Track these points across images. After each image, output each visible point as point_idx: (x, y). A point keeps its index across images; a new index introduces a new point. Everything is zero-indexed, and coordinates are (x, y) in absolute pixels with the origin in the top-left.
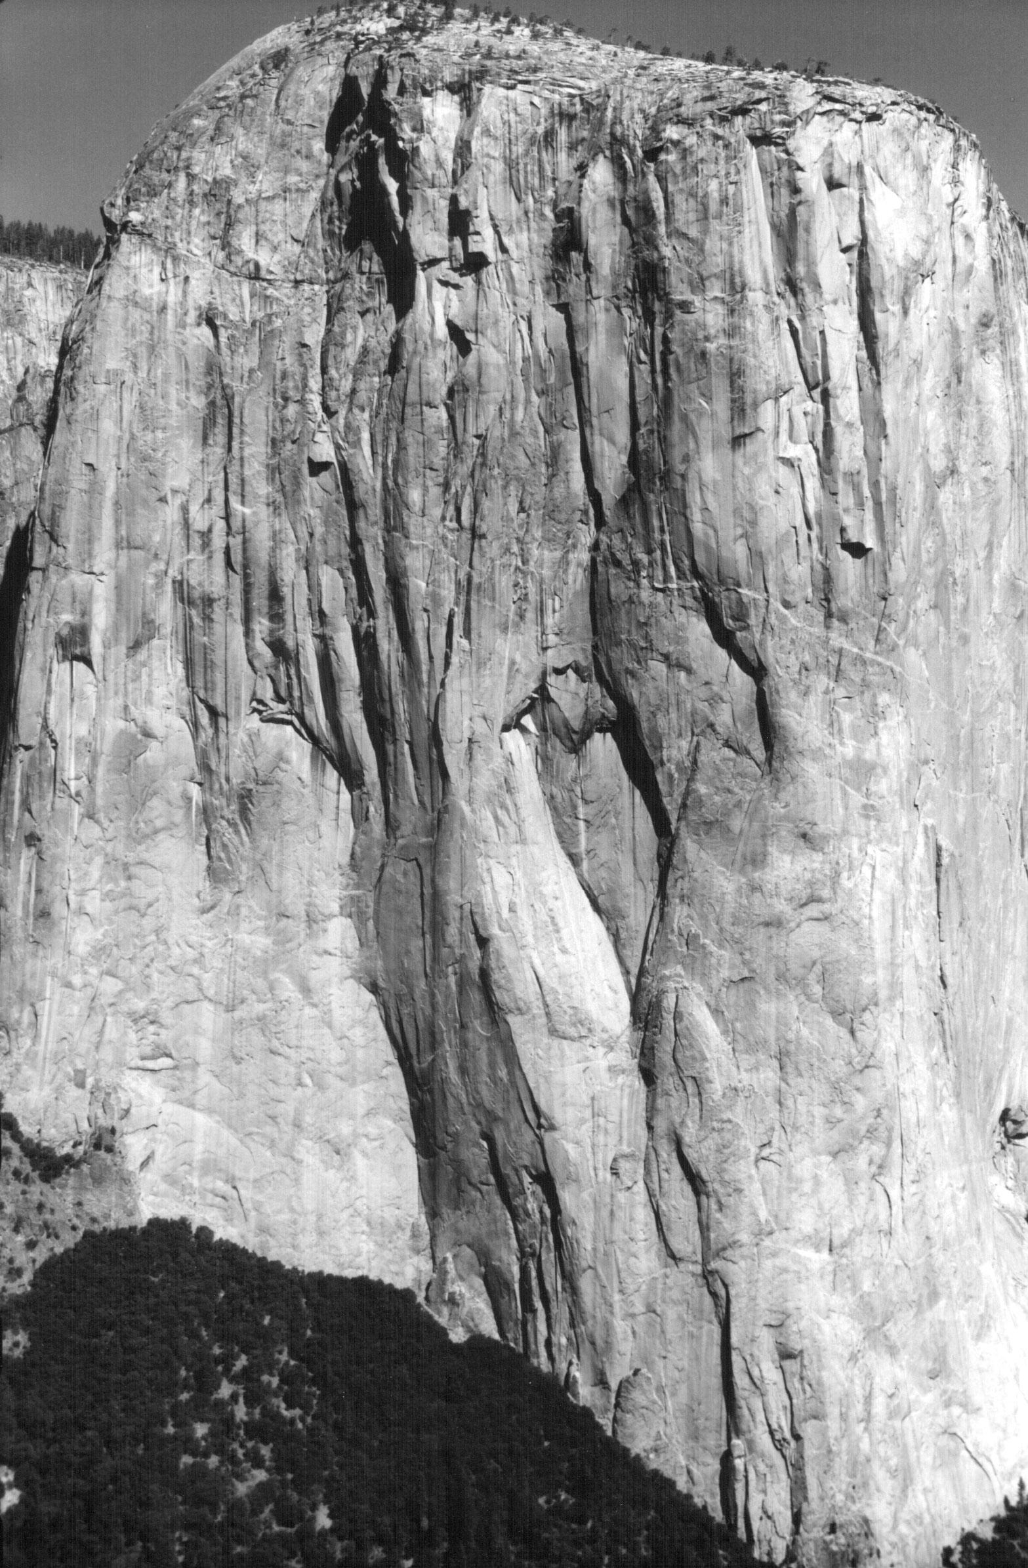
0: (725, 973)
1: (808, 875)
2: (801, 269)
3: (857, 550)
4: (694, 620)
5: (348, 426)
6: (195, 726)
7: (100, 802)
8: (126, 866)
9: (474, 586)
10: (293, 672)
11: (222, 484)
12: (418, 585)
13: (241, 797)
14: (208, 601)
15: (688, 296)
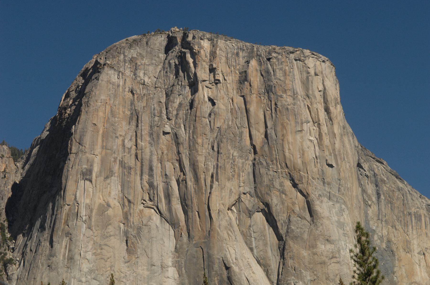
0: (309, 278)
1: (331, 250)
2: (310, 92)
3: (331, 166)
4: (286, 181)
5: (176, 123)
6: (123, 206)
7: (93, 224)
8: (100, 245)
9: (219, 167)
10: (155, 192)
11: (135, 136)
12: (201, 165)
13: (138, 229)
14: (130, 168)
15: (281, 94)
